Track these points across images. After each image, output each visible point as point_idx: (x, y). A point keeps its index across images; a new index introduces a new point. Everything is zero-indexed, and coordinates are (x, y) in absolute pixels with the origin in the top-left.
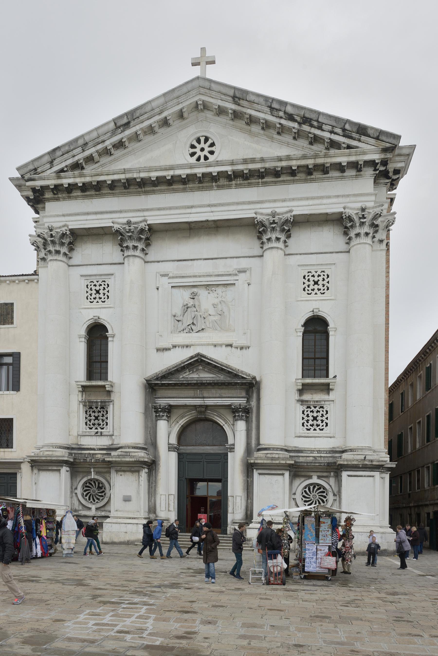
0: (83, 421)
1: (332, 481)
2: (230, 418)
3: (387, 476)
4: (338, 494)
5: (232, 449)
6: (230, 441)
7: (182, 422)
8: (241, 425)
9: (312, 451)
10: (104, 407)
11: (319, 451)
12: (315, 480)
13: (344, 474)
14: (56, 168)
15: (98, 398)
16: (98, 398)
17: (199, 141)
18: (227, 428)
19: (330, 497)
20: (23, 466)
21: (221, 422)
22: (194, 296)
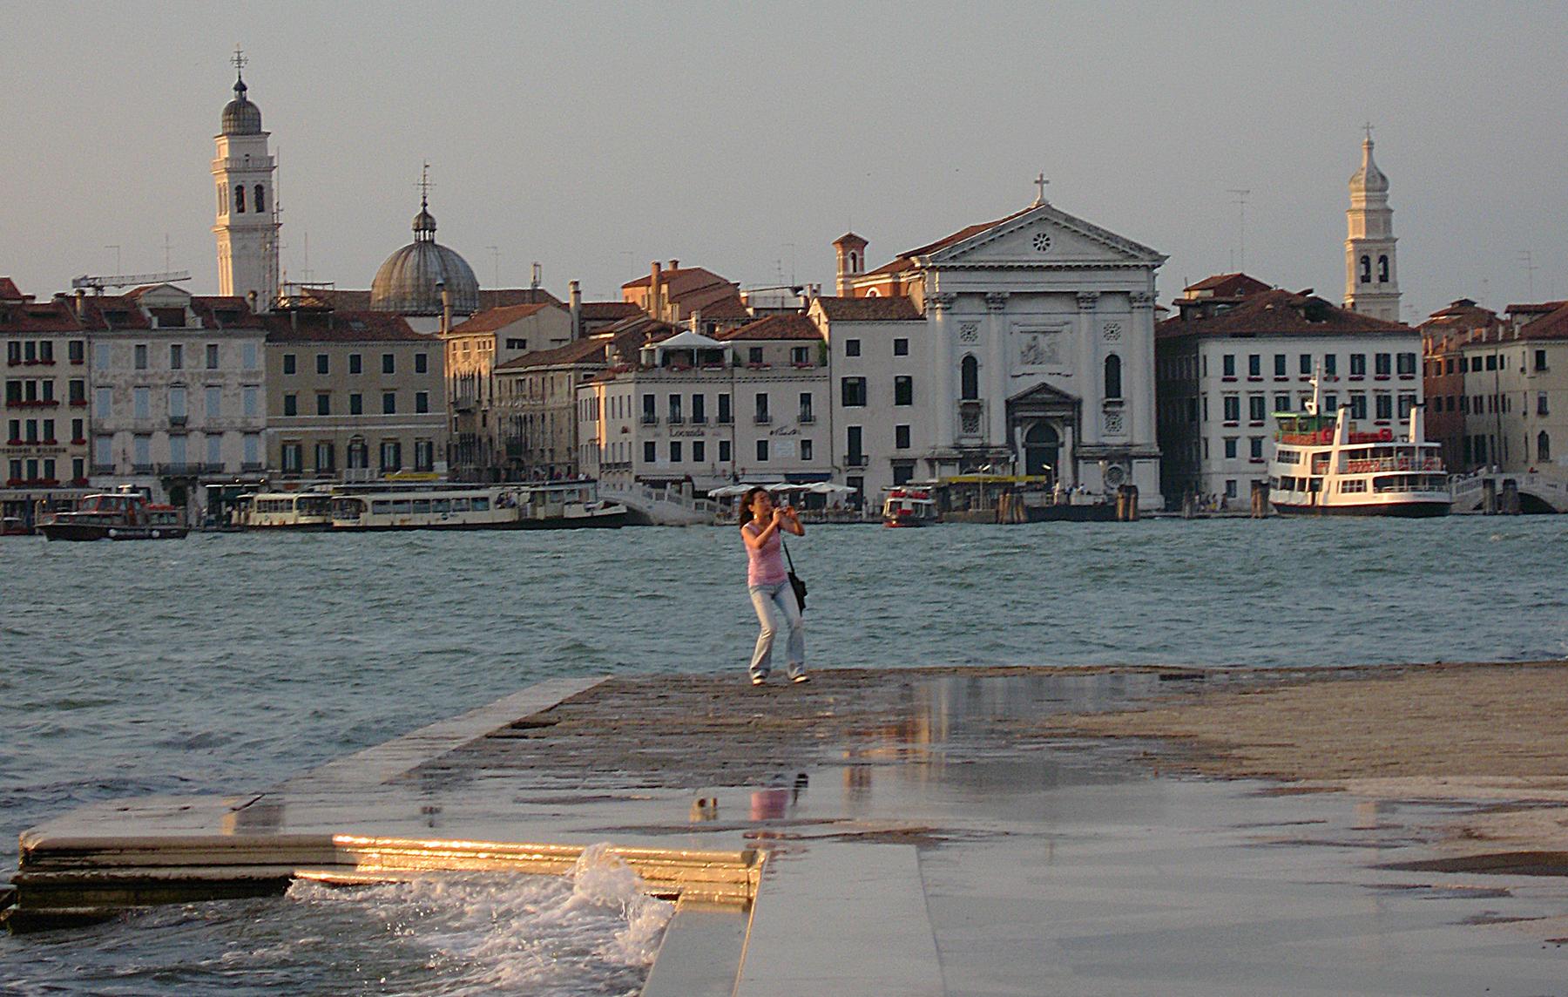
0: (961, 427)
1: (1126, 465)
2: (1061, 424)
3: (1158, 461)
4: (1130, 473)
5: (1063, 445)
6: (1061, 440)
7: (1030, 427)
8: (1069, 429)
9: (1112, 446)
10: (976, 417)
11: (1118, 446)
12: (1115, 465)
13: (1135, 461)
14: (951, 255)
15: (972, 411)
16: (972, 411)
17: (1039, 235)
18: (1059, 431)
19: (1125, 476)
20: (918, 461)
21: (1055, 426)
22: (1035, 338)
